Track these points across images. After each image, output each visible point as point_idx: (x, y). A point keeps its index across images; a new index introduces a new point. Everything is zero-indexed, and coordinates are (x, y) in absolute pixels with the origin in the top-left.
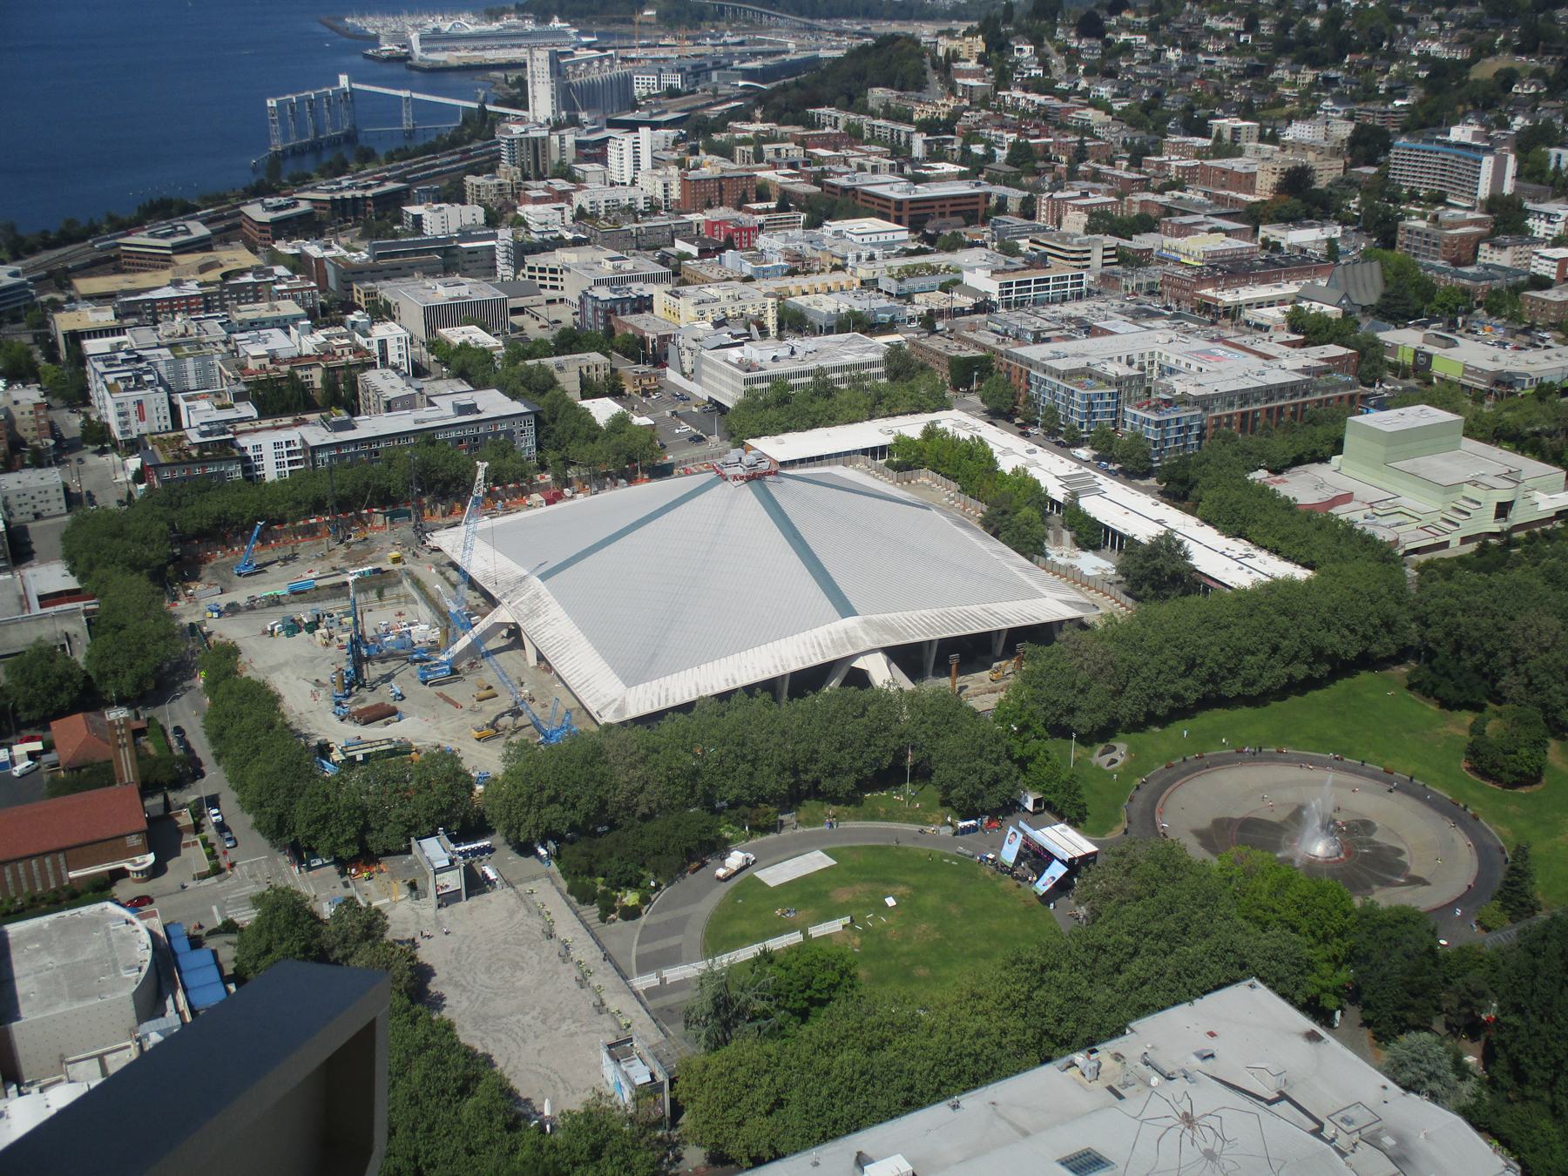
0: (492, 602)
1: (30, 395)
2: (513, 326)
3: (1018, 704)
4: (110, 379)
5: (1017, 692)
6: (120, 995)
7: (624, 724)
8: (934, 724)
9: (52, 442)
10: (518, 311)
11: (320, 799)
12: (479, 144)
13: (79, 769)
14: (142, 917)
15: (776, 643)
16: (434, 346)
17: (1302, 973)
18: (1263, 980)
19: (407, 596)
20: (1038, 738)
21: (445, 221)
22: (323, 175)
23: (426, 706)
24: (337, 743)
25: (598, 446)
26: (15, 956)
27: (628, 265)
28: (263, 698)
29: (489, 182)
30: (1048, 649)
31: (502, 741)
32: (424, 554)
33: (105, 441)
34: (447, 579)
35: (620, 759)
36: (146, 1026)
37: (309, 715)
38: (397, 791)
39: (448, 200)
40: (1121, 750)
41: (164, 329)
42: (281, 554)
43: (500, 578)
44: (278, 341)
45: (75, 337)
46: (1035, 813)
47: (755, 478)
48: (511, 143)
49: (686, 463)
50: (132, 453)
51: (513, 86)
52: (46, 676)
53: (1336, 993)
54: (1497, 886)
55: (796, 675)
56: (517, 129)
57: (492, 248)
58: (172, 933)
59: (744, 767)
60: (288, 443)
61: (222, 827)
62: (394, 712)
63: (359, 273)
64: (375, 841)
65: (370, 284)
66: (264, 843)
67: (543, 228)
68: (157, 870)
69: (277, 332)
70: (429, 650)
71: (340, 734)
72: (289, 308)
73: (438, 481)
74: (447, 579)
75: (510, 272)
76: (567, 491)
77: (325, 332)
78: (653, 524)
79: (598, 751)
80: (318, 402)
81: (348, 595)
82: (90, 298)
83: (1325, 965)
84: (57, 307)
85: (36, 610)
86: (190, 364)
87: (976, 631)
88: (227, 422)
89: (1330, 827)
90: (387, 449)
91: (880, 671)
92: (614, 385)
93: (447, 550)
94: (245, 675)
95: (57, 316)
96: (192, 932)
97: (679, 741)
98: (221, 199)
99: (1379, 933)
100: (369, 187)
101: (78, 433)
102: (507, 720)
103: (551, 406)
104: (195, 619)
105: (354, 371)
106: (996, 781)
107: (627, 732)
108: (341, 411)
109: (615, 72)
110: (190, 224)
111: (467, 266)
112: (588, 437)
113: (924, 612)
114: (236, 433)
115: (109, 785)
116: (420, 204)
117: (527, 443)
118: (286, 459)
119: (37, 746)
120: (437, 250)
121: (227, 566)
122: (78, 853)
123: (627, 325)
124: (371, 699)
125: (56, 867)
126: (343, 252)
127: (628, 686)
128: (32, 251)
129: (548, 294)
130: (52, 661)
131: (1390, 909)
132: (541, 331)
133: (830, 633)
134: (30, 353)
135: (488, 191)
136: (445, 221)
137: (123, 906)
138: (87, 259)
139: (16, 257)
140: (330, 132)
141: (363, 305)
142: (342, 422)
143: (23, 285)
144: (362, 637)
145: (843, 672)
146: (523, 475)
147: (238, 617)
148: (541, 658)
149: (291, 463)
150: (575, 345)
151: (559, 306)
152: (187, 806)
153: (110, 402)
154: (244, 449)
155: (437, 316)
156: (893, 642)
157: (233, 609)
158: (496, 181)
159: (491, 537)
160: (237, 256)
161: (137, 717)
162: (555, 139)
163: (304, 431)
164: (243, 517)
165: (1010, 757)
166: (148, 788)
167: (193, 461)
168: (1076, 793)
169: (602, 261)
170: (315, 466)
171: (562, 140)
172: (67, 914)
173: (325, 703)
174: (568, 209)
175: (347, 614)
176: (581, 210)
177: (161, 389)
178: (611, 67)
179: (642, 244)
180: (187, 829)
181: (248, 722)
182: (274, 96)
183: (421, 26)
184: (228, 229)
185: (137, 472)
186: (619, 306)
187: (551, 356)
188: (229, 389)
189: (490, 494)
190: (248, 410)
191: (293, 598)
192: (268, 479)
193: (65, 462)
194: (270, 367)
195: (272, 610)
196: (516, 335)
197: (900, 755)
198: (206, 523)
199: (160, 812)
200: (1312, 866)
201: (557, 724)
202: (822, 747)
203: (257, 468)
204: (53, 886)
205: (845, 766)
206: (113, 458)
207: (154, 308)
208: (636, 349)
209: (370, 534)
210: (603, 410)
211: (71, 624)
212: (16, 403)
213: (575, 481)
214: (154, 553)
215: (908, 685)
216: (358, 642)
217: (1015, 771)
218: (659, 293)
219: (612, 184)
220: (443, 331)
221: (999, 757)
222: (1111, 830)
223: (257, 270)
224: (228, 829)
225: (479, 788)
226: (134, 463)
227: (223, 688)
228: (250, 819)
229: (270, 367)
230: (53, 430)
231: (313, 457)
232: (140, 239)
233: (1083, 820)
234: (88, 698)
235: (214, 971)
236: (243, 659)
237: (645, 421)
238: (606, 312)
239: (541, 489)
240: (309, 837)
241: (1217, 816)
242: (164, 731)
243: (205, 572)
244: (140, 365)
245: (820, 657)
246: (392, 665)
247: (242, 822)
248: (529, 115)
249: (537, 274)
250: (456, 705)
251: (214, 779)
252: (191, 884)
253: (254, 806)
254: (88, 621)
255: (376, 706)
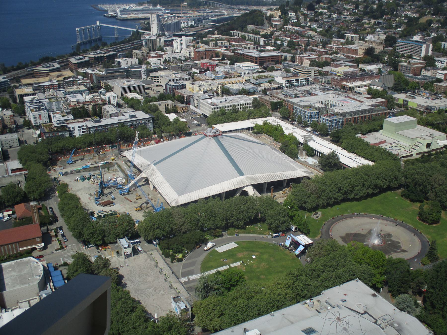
0: (140, 172)
1: (8, 113)
2: (146, 93)
3: (290, 201)
4: (31, 108)
5: (290, 197)
6: (34, 283)
7: (178, 206)
8: (266, 206)
9: (15, 126)
10: (148, 89)
11: (91, 228)
12: (137, 41)
13: (22, 219)
14: (40, 261)
15: (221, 183)
16: (124, 98)
19: (116, 170)
20: (296, 210)
21: (127, 63)
22: (92, 50)
23: (121, 201)
24: (96, 212)
25: (170, 127)
26: (4, 272)
27: (179, 76)
28: (75, 199)
29: (139, 52)
30: (299, 185)
31: (143, 211)
32: (121, 158)
33: (30, 126)
34: (128, 165)
35: (177, 216)
36: (42, 292)
37: (88, 204)
38: (113, 225)
39: (128, 57)
40: (320, 214)
41: (47, 94)
42: (80, 158)
43: (143, 165)
44: (79, 97)
45: (21, 96)
46: (295, 232)
47: (215, 136)
48: (146, 41)
49: (195, 132)
50: (38, 129)
51: (146, 24)
52: (13, 193)
54: (427, 252)
55: (227, 192)
56: (147, 37)
57: (140, 71)
58: (49, 266)
59: (212, 218)
60: (82, 126)
61: (63, 236)
62: (112, 203)
63: (102, 78)
64: (107, 240)
65: (106, 81)
66: (75, 240)
67: (155, 65)
68: (45, 248)
69: (79, 95)
70: (122, 185)
71: (97, 209)
72: (82, 88)
73: (125, 137)
74: (128, 165)
75: (145, 78)
76: (162, 140)
77: (93, 94)
78: (186, 149)
79: (170, 214)
80: (91, 114)
81: (99, 169)
82: (26, 85)
84: (16, 87)
85: (10, 174)
86: (54, 104)
87: (278, 180)
88: (65, 120)
89: (379, 236)
90: (110, 128)
91: (251, 191)
92: (175, 110)
93: (127, 157)
94: (70, 192)
95: (16, 90)
96: (55, 266)
97: (194, 211)
98: (63, 57)
99: (393, 266)
100: (105, 53)
101: (22, 123)
102: (145, 205)
103: (157, 116)
104: (56, 176)
105: (101, 106)
106: (284, 222)
107: (179, 209)
108: (97, 117)
109: (175, 20)
110: (54, 64)
111: (133, 76)
112: (168, 124)
113: (263, 174)
114: (67, 123)
115: (31, 224)
116: (120, 58)
117: (150, 126)
118: (82, 131)
119: (11, 212)
120: (124, 71)
121: (65, 161)
122: (22, 243)
123: (179, 93)
124: (106, 199)
125: (16, 247)
126: (98, 72)
127: (179, 196)
128: (9, 71)
129: (156, 84)
130: (15, 188)
132: (154, 94)
133: (237, 180)
134: (8, 101)
135: (139, 54)
136: (127, 63)
137: (35, 258)
138: (25, 74)
139: (5, 73)
140: (94, 38)
141: (103, 87)
142: (97, 120)
143: (6, 81)
144: (103, 181)
145: (240, 192)
146: (149, 135)
147: (68, 176)
148: (154, 187)
149: (83, 132)
150: (164, 98)
151: (159, 87)
152: (53, 229)
153: (31, 115)
154: (69, 128)
155: (125, 90)
156: (255, 183)
157: (66, 173)
158: (141, 52)
159: (140, 153)
160: (67, 73)
161: (39, 204)
162: (158, 40)
163: (87, 123)
164: (69, 147)
165: (288, 216)
166: (42, 224)
167: (55, 131)
168: (307, 226)
169: (172, 74)
170: (90, 133)
171: (160, 40)
172: (19, 260)
173: (93, 200)
174: (162, 59)
175: (99, 175)
176: (166, 60)
177: (46, 111)
178: (174, 19)
179: (183, 69)
180: (53, 236)
181: (71, 206)
182: (78, 27)
183: (120, 7)
184: (65, 65)
185: (39, 134)
186: (176, 87)
187: (157, 101)
188: (65, 111)
189: (140, 141)
190: (71, 117)
191: (84, 170)
192: (76, 136)
193: (19, 132)
194: (77, 105)
195: (77, 174)
196: (147, 95)
197: (256, 215)
198: (59, 149)
199: (46, 231)
200: (374, 247)
201: (159, 206)
202: (234, 213)
203: (73, 133)
204: (15, 252)
205: (241, 218)
206: (32, 131)
207: (44, 88)
208: (181, 99)
209: (105, 152)
210: (172, 117)
211: (20, 178)
212: (5, 115)
213: (164, 137)
214: (44, 158)
215: (259, 195)
216: (102, 183)
217: (289, 219)
218: (188, 84)
219: (175, 52)
220: (126, 94)
221: (285, 216)
222: (317, 236)
223: (73, 77)
224: (65, 236)
225: (137, 224)
226: (38, 132)
227: (63, 196)
228: (71, 233)
229: (77, 105)
230: (15, 123)
231: (89, 130)
232: (40, 68)
233: (309, 234)
234: (25, 199)
235: (61, 277)
236: (69, 188)
237: (184, 120)
238: (173, 89)
239: (154, 139)
240: (88, 239)
241: (347, 232)
242: (47, 208)
243: (59, 163)
244: (40, 104)
245: (234, 187)
246: (112, 189)
247: (69, 234)
248: (151, 33)
249: (153, 78)
250: (130, 201)
251: (61, 222)
252: (55, 252)
253: (72, 229)
254: (25, 177)
255: (107, 201)
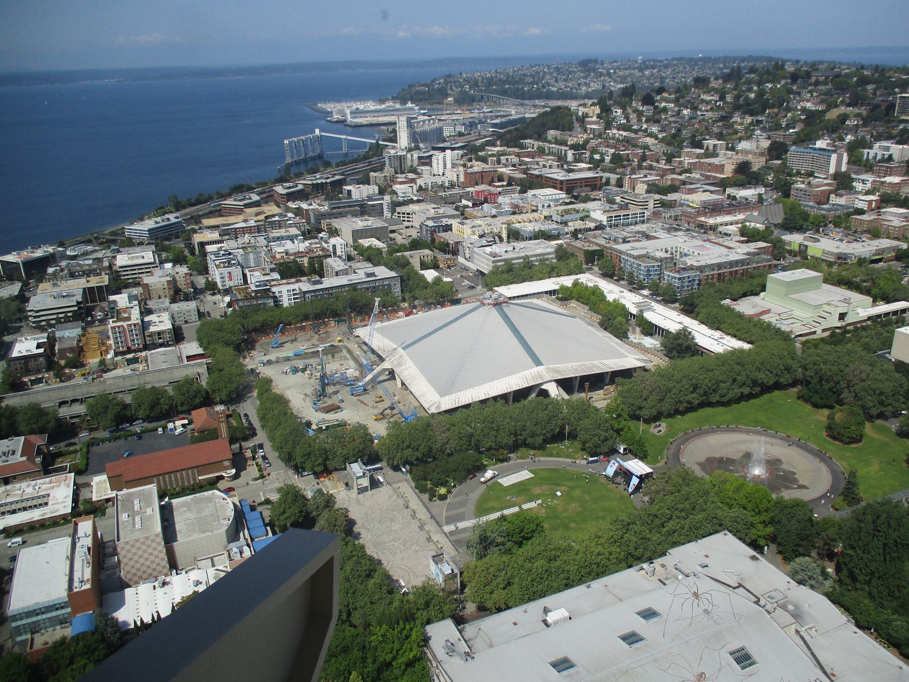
0: (382, 359)
3: (616, 405)
5: (616, 399)
7: (440, 413)
17: (748, 528)
18: (730, 531)
25: (428, 290)
30: (629, 380)
31: (386, 421)
40: (663, 426)
46: (624, 454)
47: (497, 304)
53: (765, 538)
79: (428, 425)
83: (759, 525)
91: (554, 390)
92: (435, 264)
102: (388, 412)
106: (606, 439)
117: (397, 290)
131: (790, 500)
145: (537, 390)
159: (381, 331)
165: (612, 429)
189: (381, 312)
197: (562, 428)
202: (528, 424)
205: (538, 433)
210: (430, 275)
215: (566, 397)
217: (615, 436)
218: (455, 223)
221: (607, 429)
233: (646, 457)
237: (449, 279)
239: (403, 310)
